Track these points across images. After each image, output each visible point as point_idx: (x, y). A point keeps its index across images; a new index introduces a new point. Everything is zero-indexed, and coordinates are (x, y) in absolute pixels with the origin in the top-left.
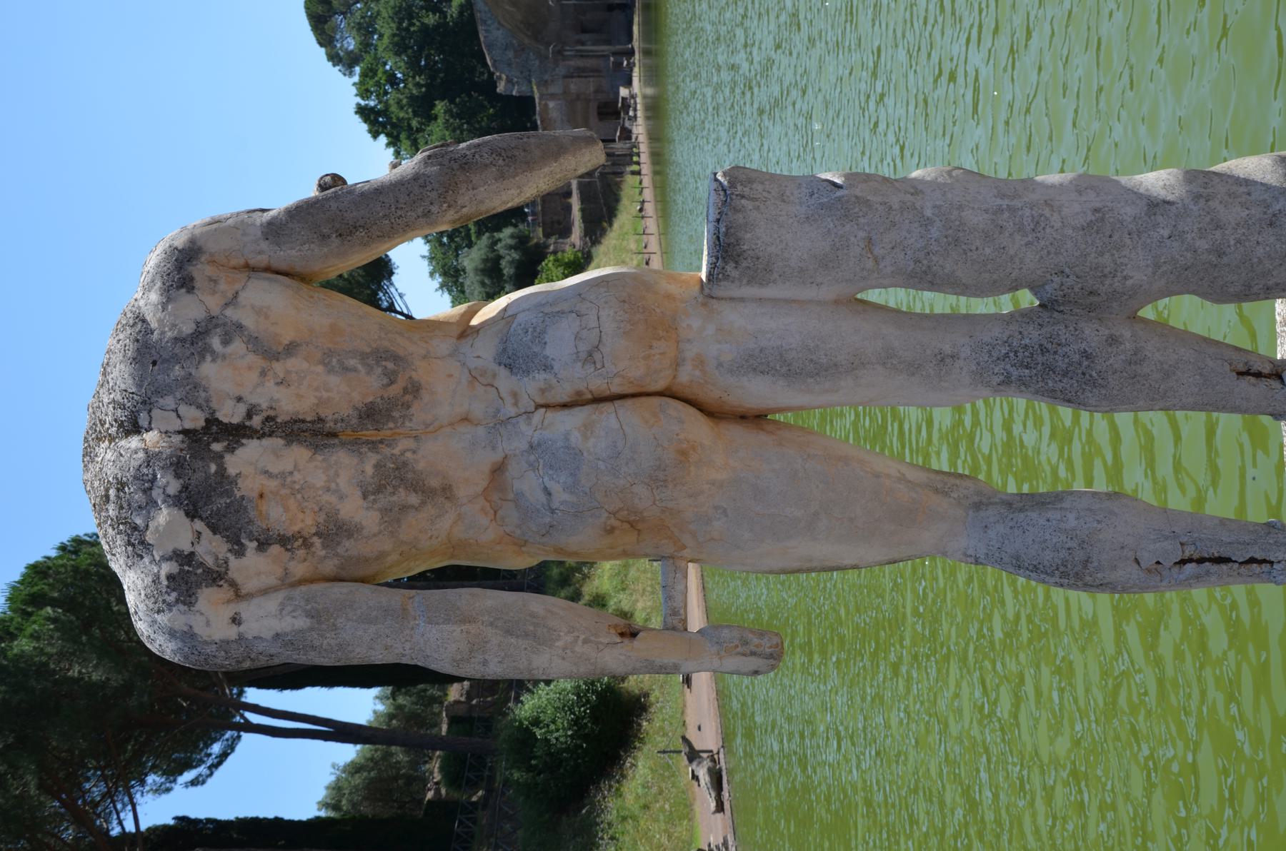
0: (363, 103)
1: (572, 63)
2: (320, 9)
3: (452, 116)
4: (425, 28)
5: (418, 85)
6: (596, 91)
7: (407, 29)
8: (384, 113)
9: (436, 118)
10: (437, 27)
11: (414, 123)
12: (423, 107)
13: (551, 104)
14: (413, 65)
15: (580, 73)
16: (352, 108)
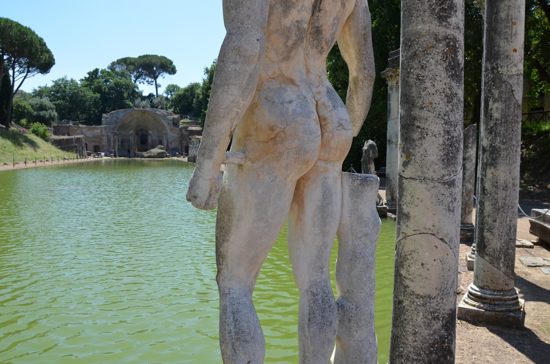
0: (99, 71)
1: (112, 138)
2: (128, 61)
3: (95, 99)
4: (123, 93)
5: (105, 89)
6: (103, 145)
7: (122, 87)
8: (96, 77)
9: (94, 93)
10: (123, 96)
11: (92, 87)
12: (98, 90)
13: (99, 131)
14: (111, 88)
15: (109, 140)
16: (98, 68)
